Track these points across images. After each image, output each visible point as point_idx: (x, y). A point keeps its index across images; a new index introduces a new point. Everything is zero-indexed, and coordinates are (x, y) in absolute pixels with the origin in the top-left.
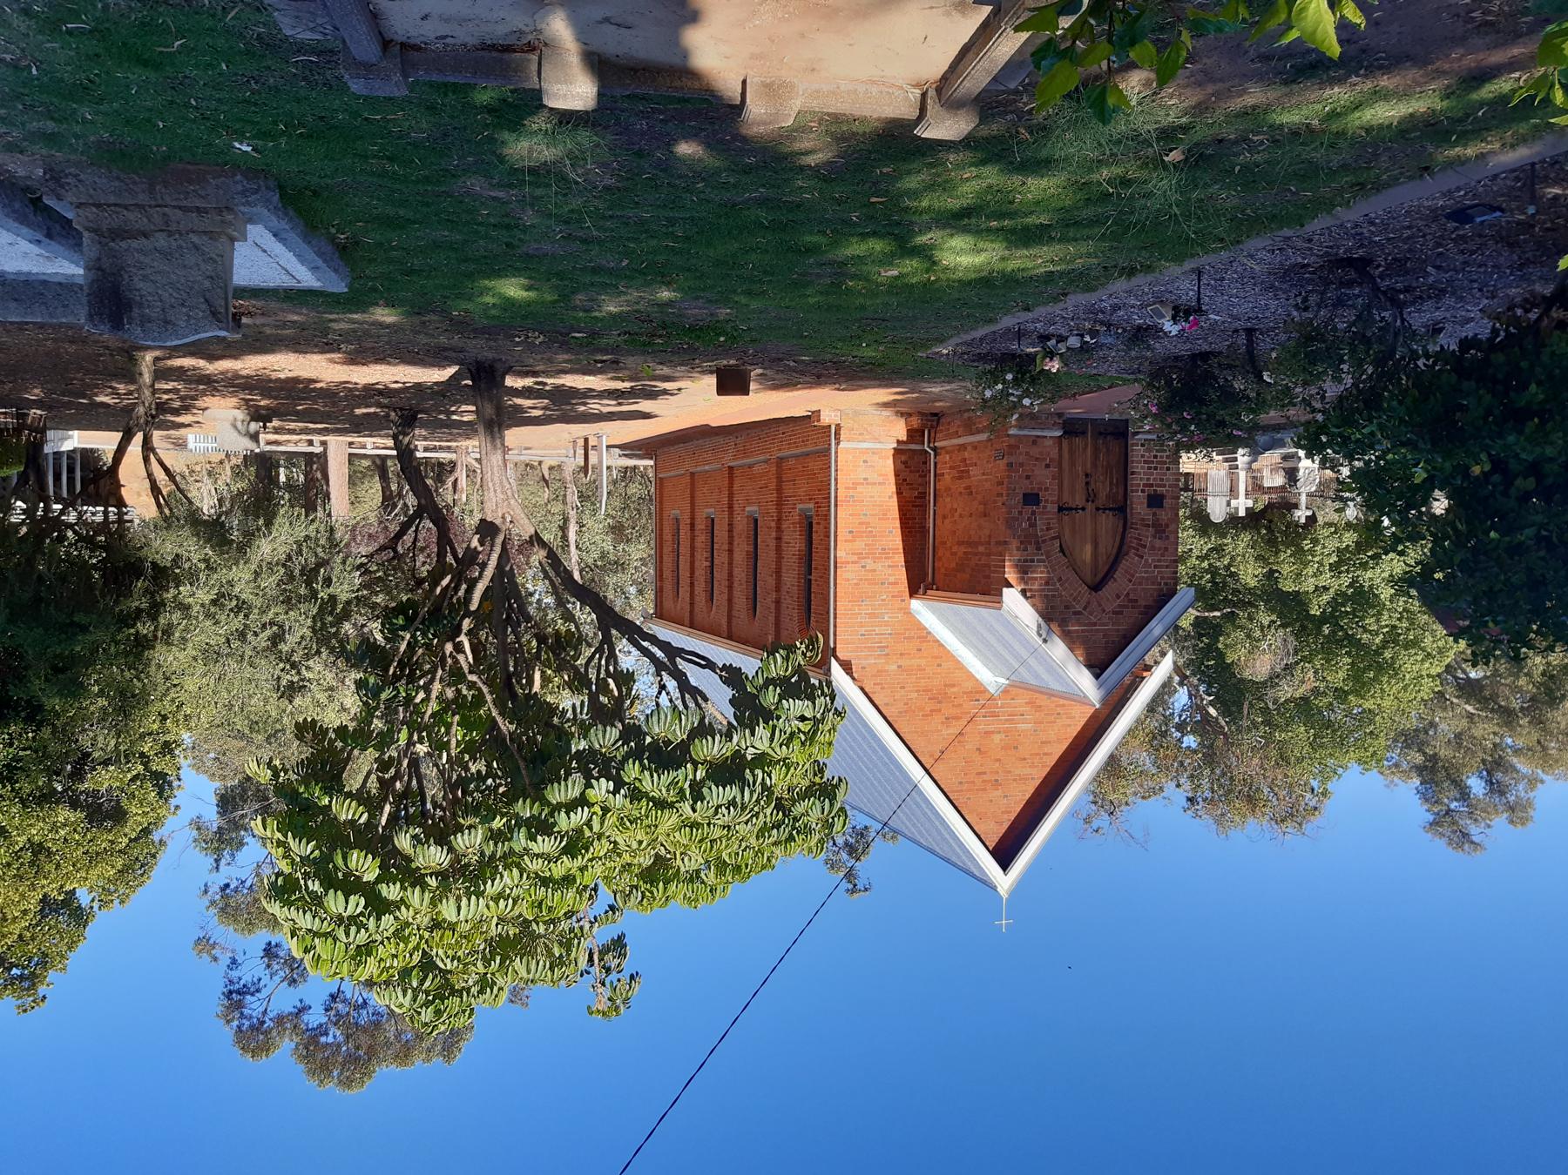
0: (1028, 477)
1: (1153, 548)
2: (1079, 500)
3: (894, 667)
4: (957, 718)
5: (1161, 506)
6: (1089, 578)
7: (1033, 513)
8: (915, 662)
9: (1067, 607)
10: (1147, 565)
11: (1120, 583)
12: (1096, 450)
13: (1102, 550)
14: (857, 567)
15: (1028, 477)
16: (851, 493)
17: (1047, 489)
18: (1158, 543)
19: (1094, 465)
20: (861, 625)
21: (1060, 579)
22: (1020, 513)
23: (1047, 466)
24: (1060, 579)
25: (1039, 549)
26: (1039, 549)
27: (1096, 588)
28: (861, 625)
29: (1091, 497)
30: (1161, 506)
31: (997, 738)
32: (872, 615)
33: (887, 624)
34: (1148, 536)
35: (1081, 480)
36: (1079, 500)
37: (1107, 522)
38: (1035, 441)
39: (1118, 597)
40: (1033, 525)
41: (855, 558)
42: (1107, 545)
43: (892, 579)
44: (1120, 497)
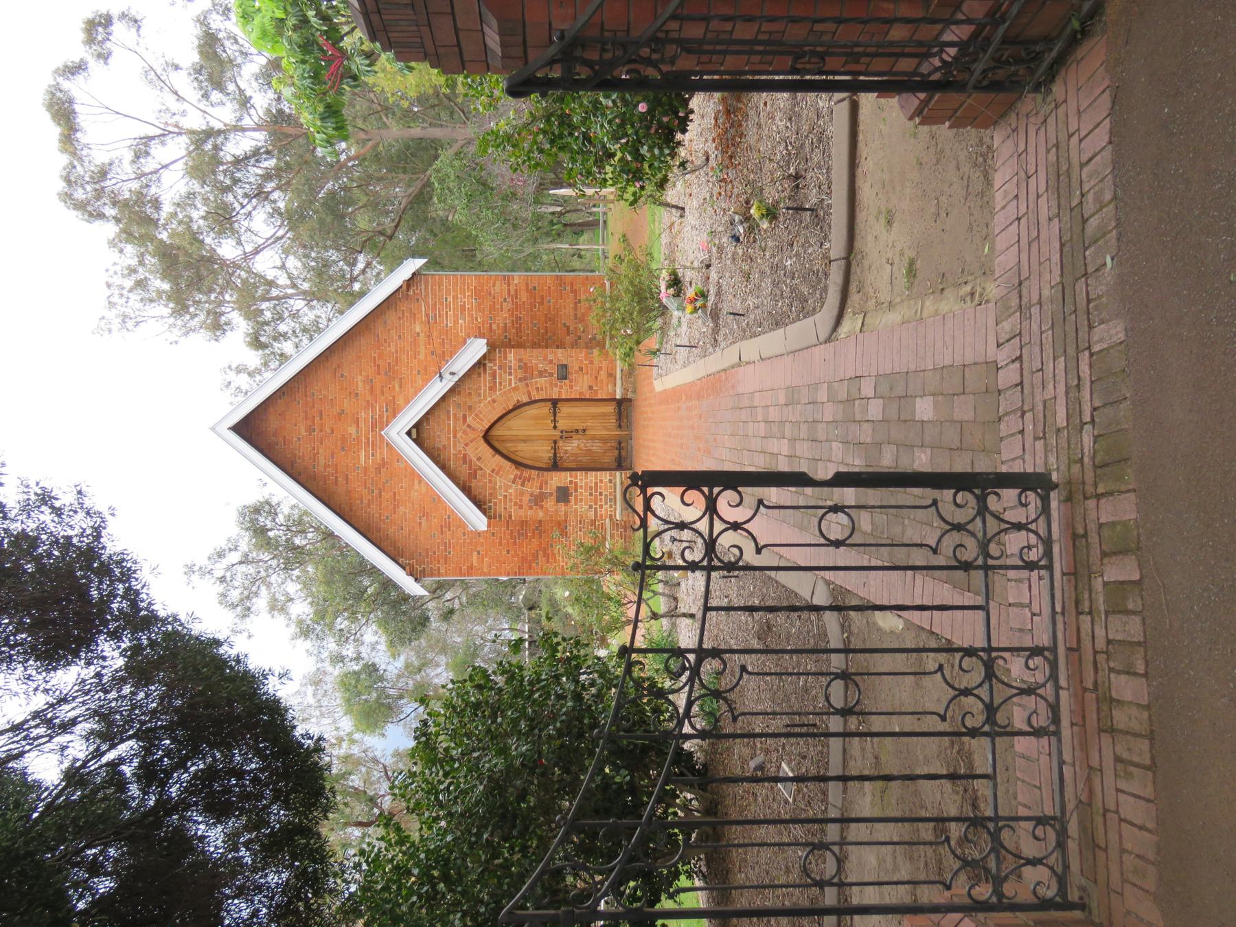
0: (581, 369)
1: (522, 494)
2: (562, 424)
3: (418, 329)
4: (372, 391)
5: (558, 501)
6: (497, 432)
7: (551, 375)
8: (422, 350)
9: (470, 408)
10: (507, 487)
11: (492, 461)
12: (604, 440)
13: (521, 446)
14: (505, 294)
15: (581, 369)
16: (568, 288)
17: (571, 387)
18: (526, 498)
19: (593, 438)
20: (455, 298)
21: (494, 401)
22: (551, 362)
23: (591, 388)
24: (494, 401)
25: (520, 380)
26: (520, 380)
27: (487, 437)
28: (455, 298)
29: (568, 435)
30: (558, 501)
31: (352, 430)
32: (463, 308)
33: (456, 322)
34: (532, 488)
35: (580, 426)
36: (562, 424)
37: (543, 452)
38: (611, 375)
39: (479, 459)
40: (541, 374)
41: (513, 292)
42: (525, 451)
43: (494, 327)
44: (566, 465)
